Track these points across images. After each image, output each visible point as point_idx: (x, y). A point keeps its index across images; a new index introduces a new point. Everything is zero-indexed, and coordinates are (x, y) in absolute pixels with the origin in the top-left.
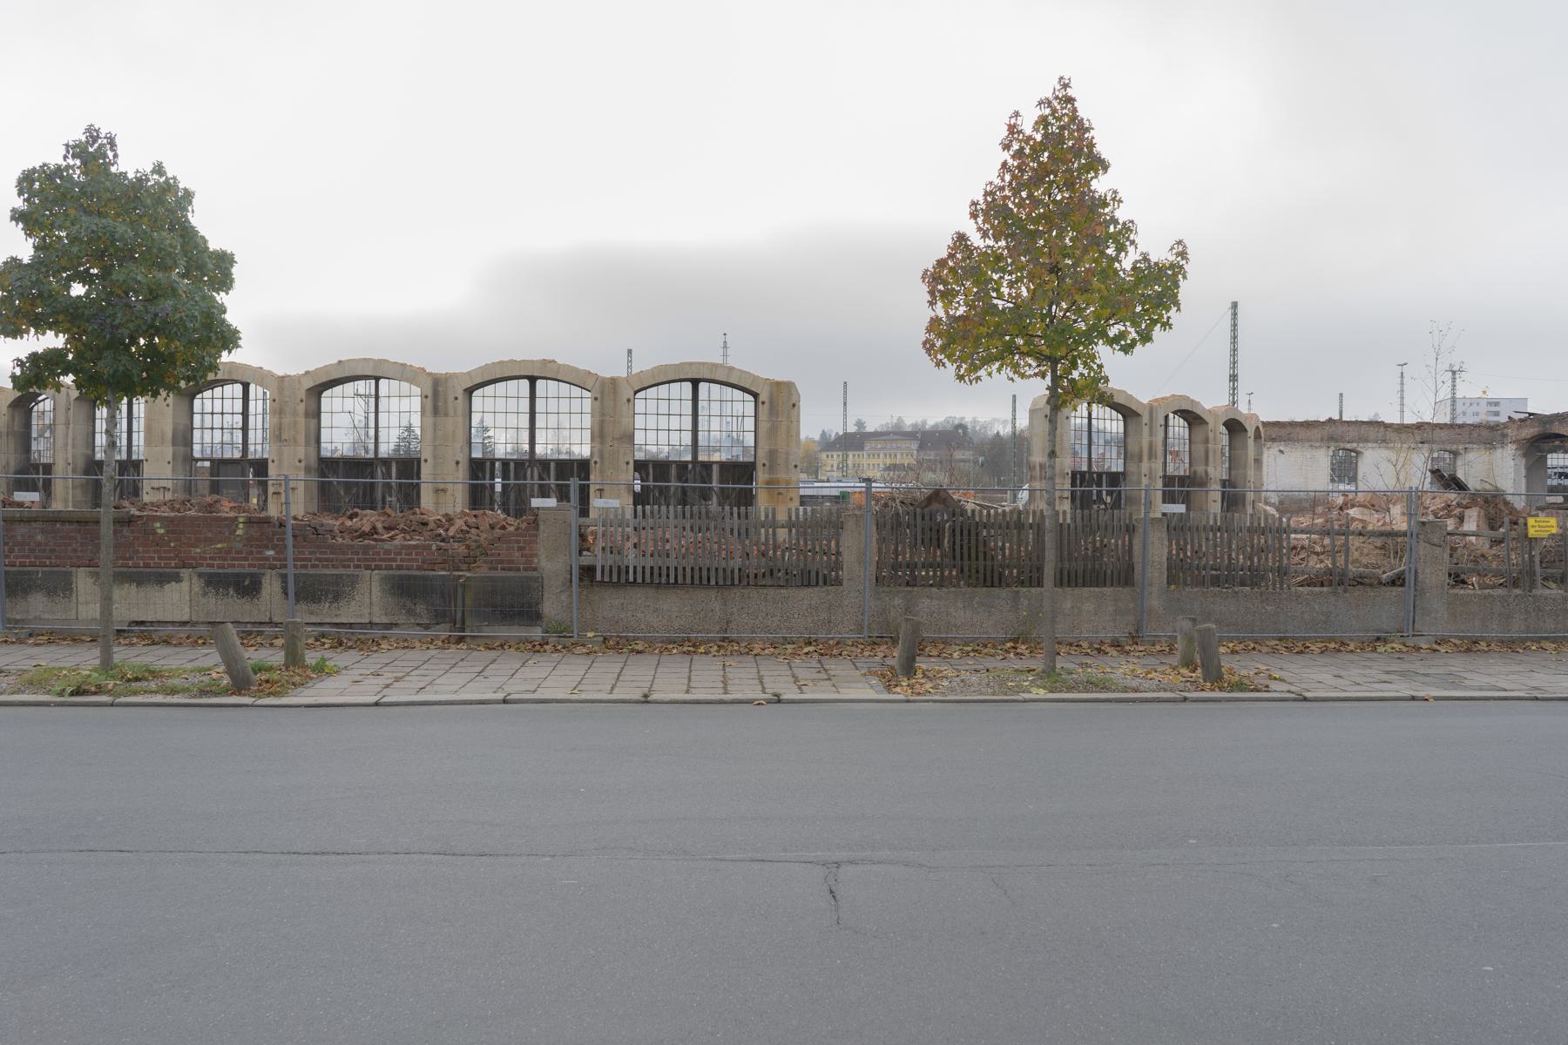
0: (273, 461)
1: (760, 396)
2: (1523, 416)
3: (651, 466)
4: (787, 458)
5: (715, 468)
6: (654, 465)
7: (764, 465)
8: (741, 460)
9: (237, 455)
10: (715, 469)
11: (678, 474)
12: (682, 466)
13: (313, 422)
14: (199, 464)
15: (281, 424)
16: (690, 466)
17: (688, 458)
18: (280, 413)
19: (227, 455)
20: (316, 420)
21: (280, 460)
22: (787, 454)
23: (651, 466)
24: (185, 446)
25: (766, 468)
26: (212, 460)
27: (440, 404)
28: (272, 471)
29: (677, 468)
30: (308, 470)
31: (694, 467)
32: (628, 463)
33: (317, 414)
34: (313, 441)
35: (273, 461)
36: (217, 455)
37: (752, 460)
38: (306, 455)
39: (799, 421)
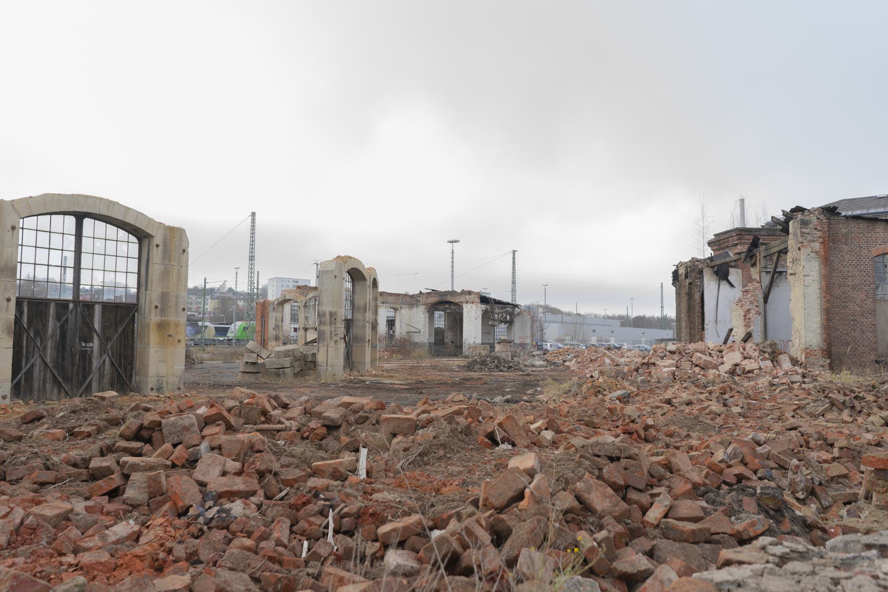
1: (155, 239)
2: (429, 291)
3: (25, 303)
4: (177, 302)
5: (98, 309)
6: (29, 303)
7: (156, 307)
8: (124, 301)
10: (98, 309)
11: (57, 313)
12: (62, 305)
16: (71, 306)
17: (69, 296)
22: (177, 297)
23: (25, 303)
25: (158, 310)
29: (56, 308)
31: (75, 307)
32: (9, 300)
37: (135, 302)
39: (187, 267)
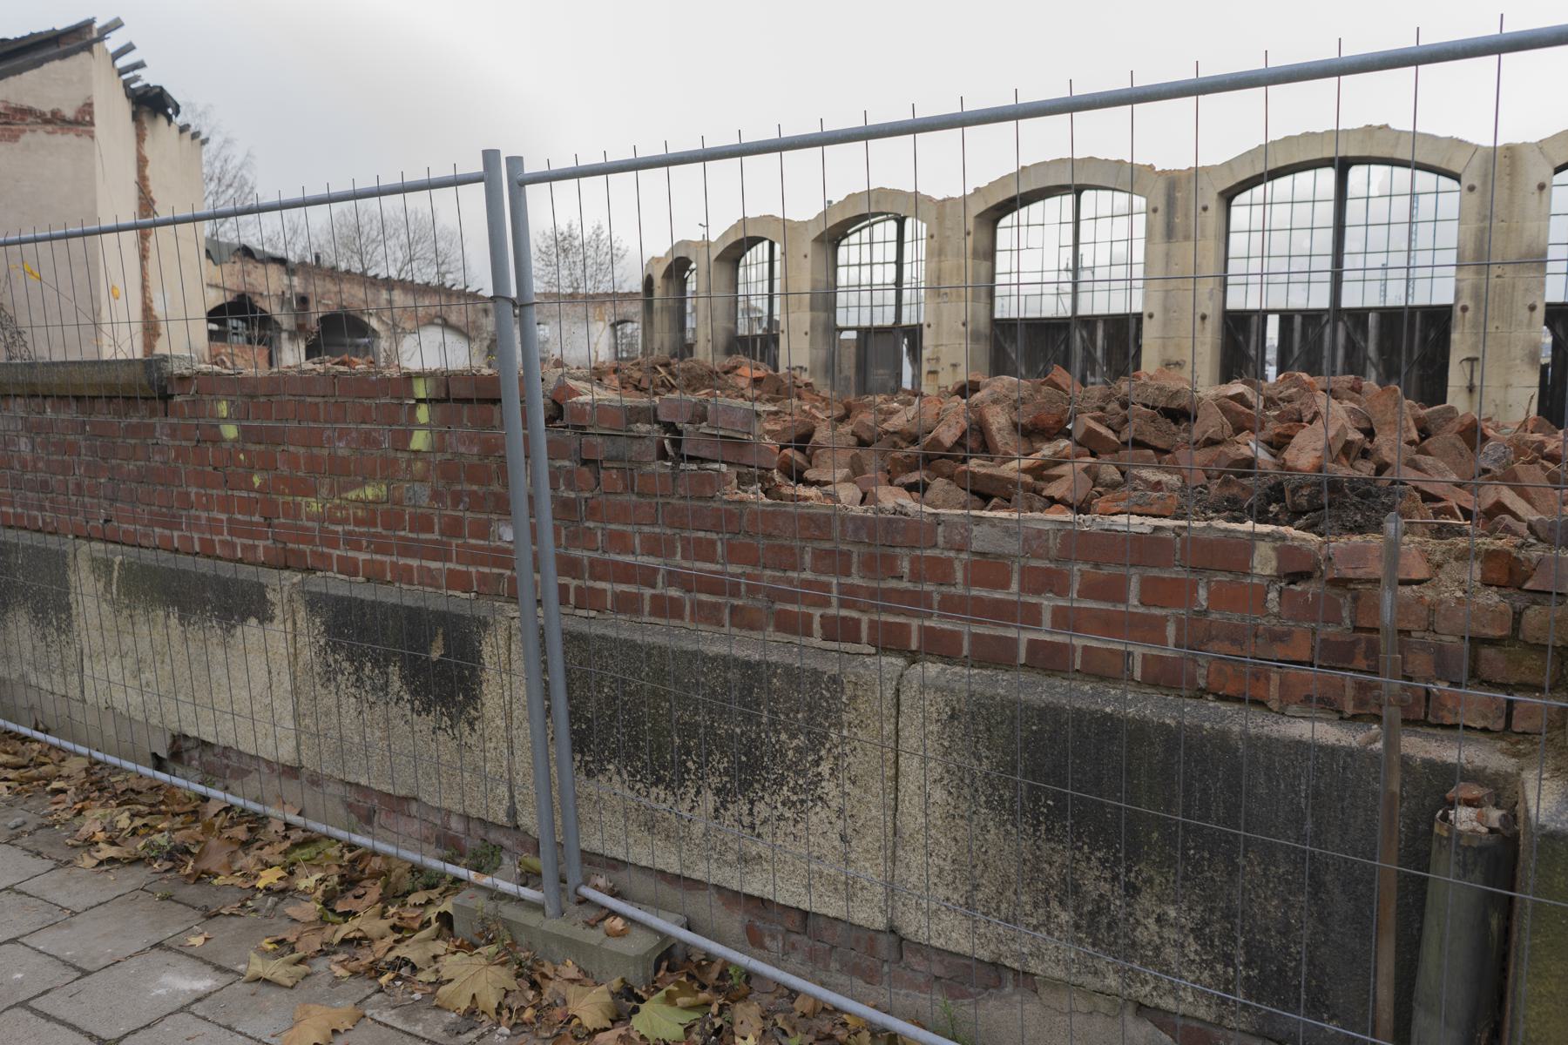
0: (929, 326)
9: (889, 320)
13: (985, 265)
14: (845, 335)
15: (940, 270)
18: (940, 255)
19: (877, 323)
20: (989, 263)
21: (939, 325)
24: (826, 311)
26: (858, 329)
27: (1177, 220)
28: (928, 339)
30: (975, 336)
33: (991, 253)
34: (983, 292)
35: (929, 326)
36: (865, 323)
38: (974, 315)
